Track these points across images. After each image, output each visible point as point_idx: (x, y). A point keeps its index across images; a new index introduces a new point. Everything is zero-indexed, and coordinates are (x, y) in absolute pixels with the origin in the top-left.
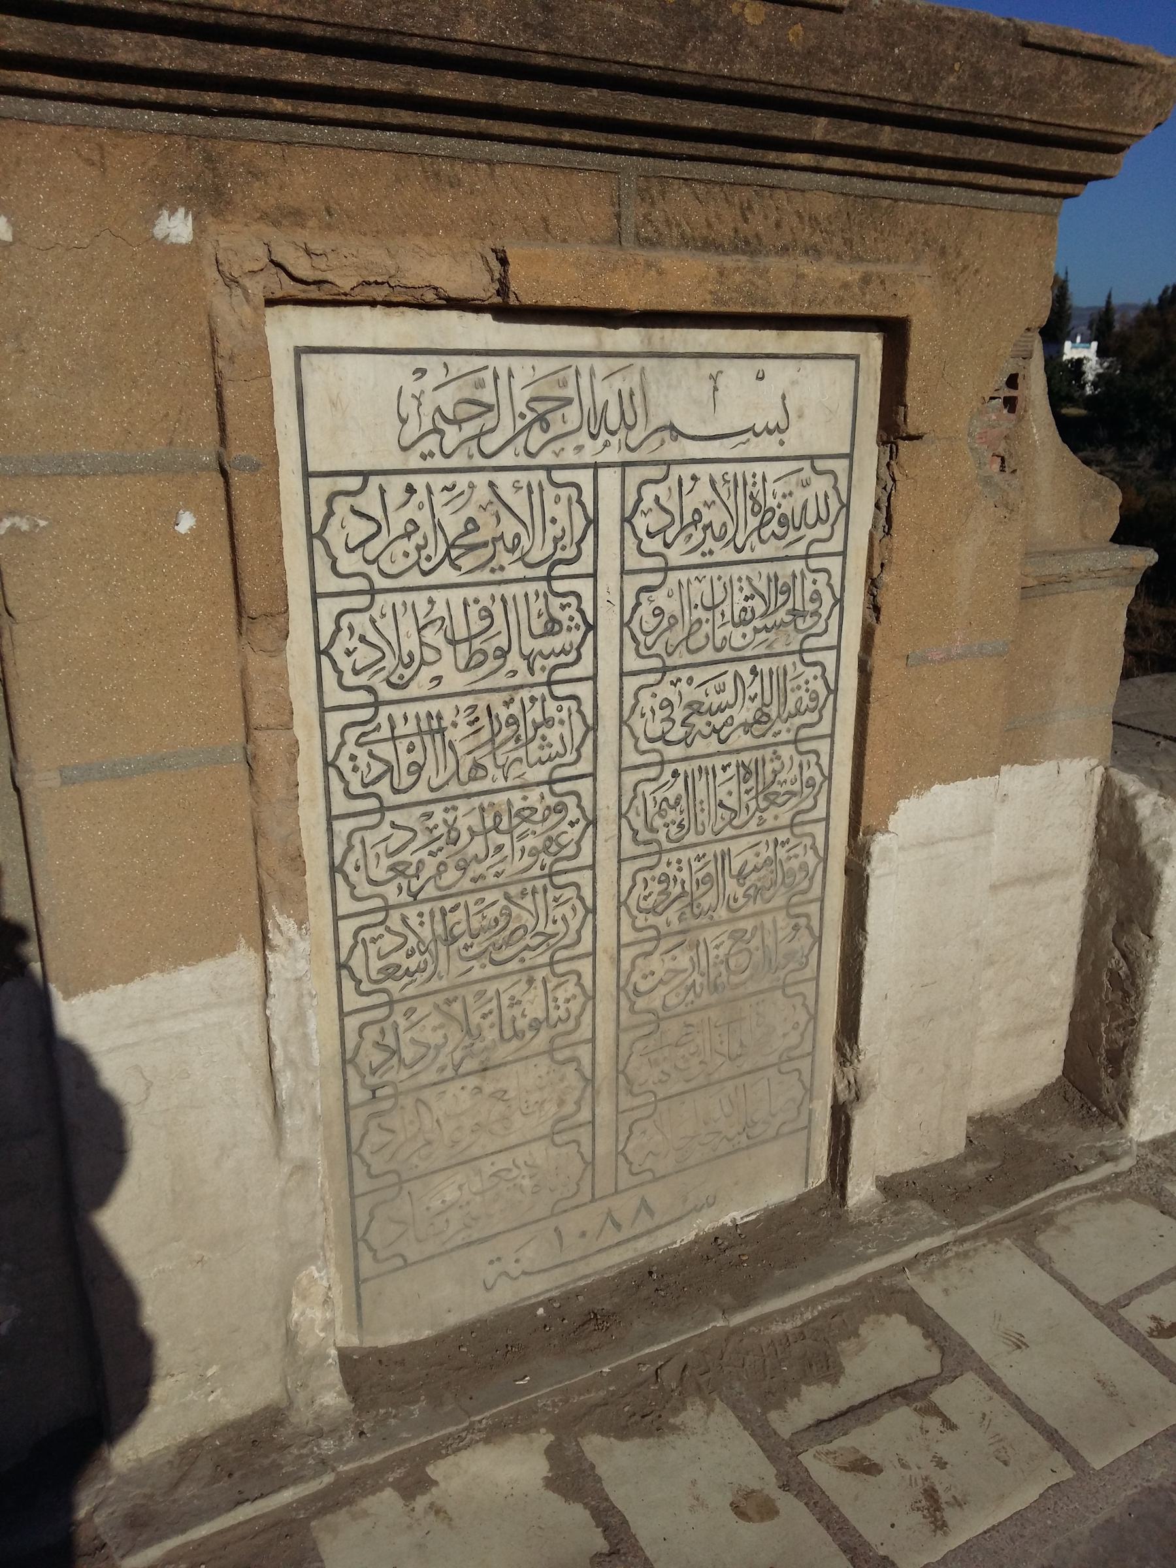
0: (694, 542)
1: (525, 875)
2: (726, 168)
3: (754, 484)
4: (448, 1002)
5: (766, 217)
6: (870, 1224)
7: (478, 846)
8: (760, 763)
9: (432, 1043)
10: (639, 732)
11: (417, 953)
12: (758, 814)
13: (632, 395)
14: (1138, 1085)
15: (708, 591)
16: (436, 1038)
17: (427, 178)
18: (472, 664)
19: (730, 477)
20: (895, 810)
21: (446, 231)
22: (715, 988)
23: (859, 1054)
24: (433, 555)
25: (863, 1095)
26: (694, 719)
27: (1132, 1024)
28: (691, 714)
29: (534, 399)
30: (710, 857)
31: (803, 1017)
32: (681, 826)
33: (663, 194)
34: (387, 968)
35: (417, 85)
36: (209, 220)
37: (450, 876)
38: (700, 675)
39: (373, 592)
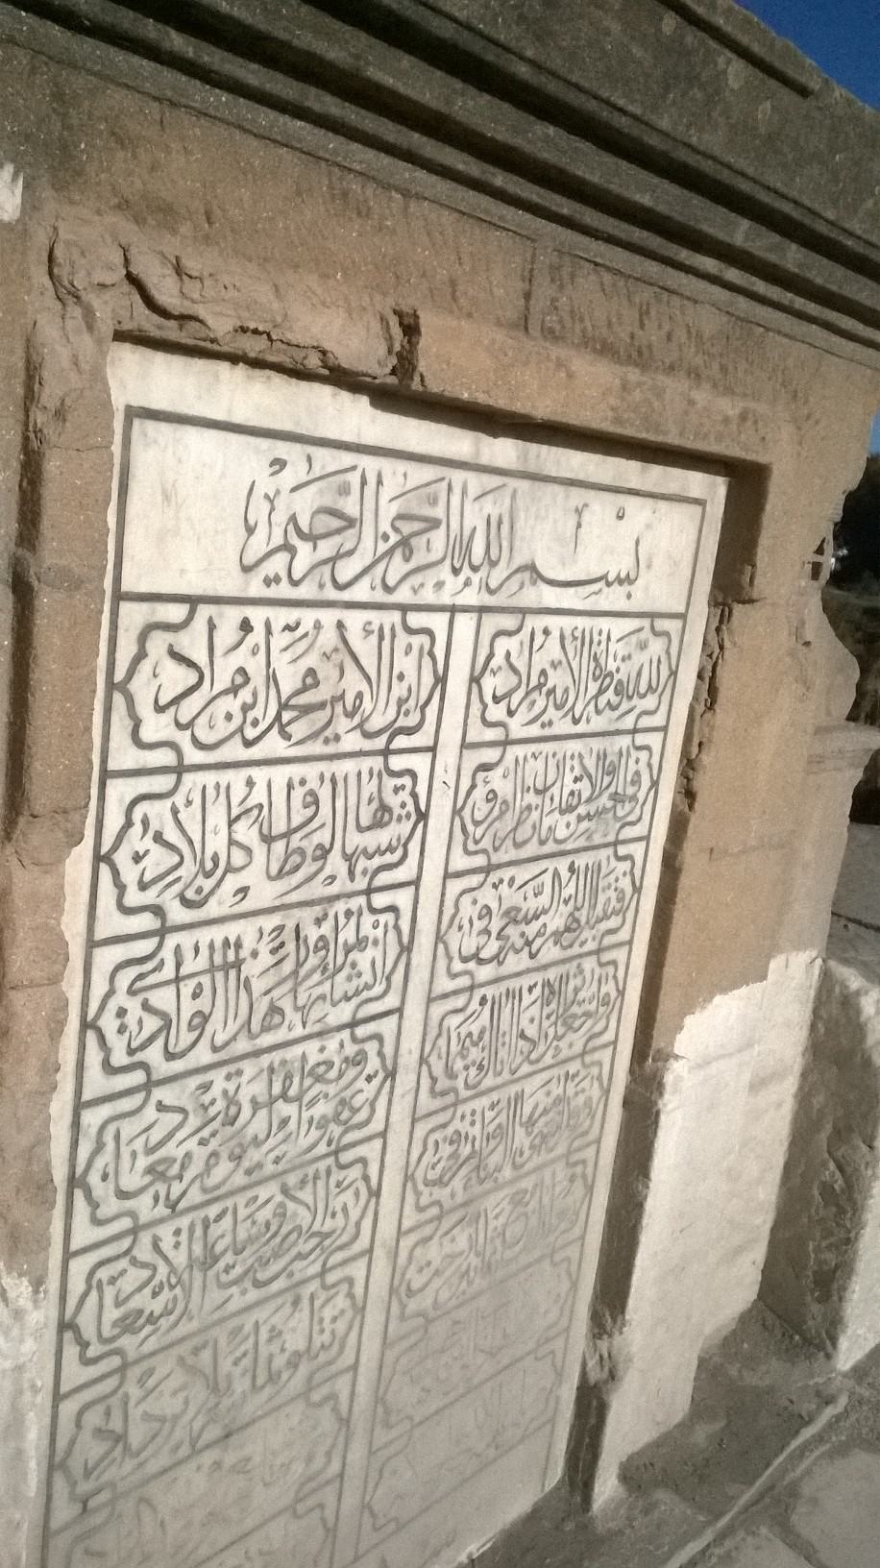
0: (537, 710)
1: (309, 1156)
2: (637, 258)
3: (599, 643)
4: (196, 1351)
5: (660, 327)
6: (621, 1532)
8: (564, 979)
9: (168, 1412)
11: (166, 1289)
12: (555, 1043)
13: (500, 523)
14: (849, 1311)
15: (541, 772)
17: (333, 197)
18: (287, 868)
19: (578, 634)
21: (345, 274)
23: (623, 1325)
24: (260, 719)
25: (620, 1373)
26: (511, 930)
27: (846, 1243)
28: (507, 925)
29: (400, 517)
30: (503, 1104)
31: (565, 1285)
32: (480, 1067)
33: (573, 276)
34: (124, 1318)
35: (368, 64)
36: (48, 193)
37: (223, 1168)
38: (522, 874)
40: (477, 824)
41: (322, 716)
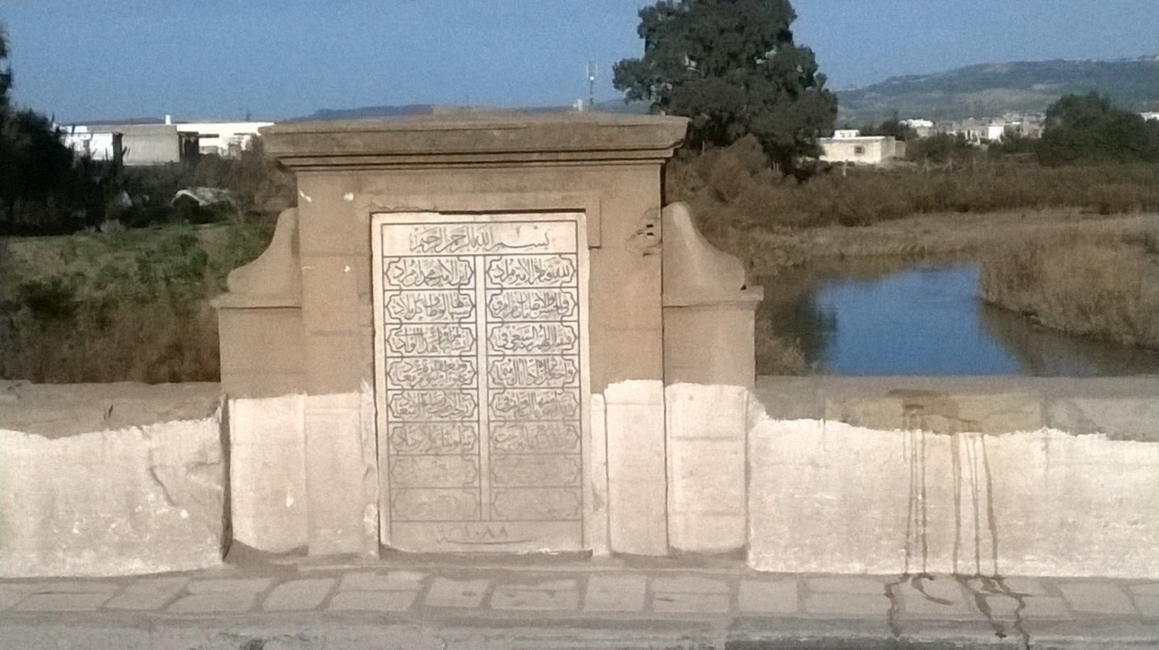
0: (513, 280)
4: (425, 427)
7: (434, 374)
10: (494, 343)
20: (607, 387)
22: (532, 447)
26: (516, 341)
32: (513, 380)
37: (424, 383)
39: (401, 290)
40: (496, 310)
41: (438, 280)
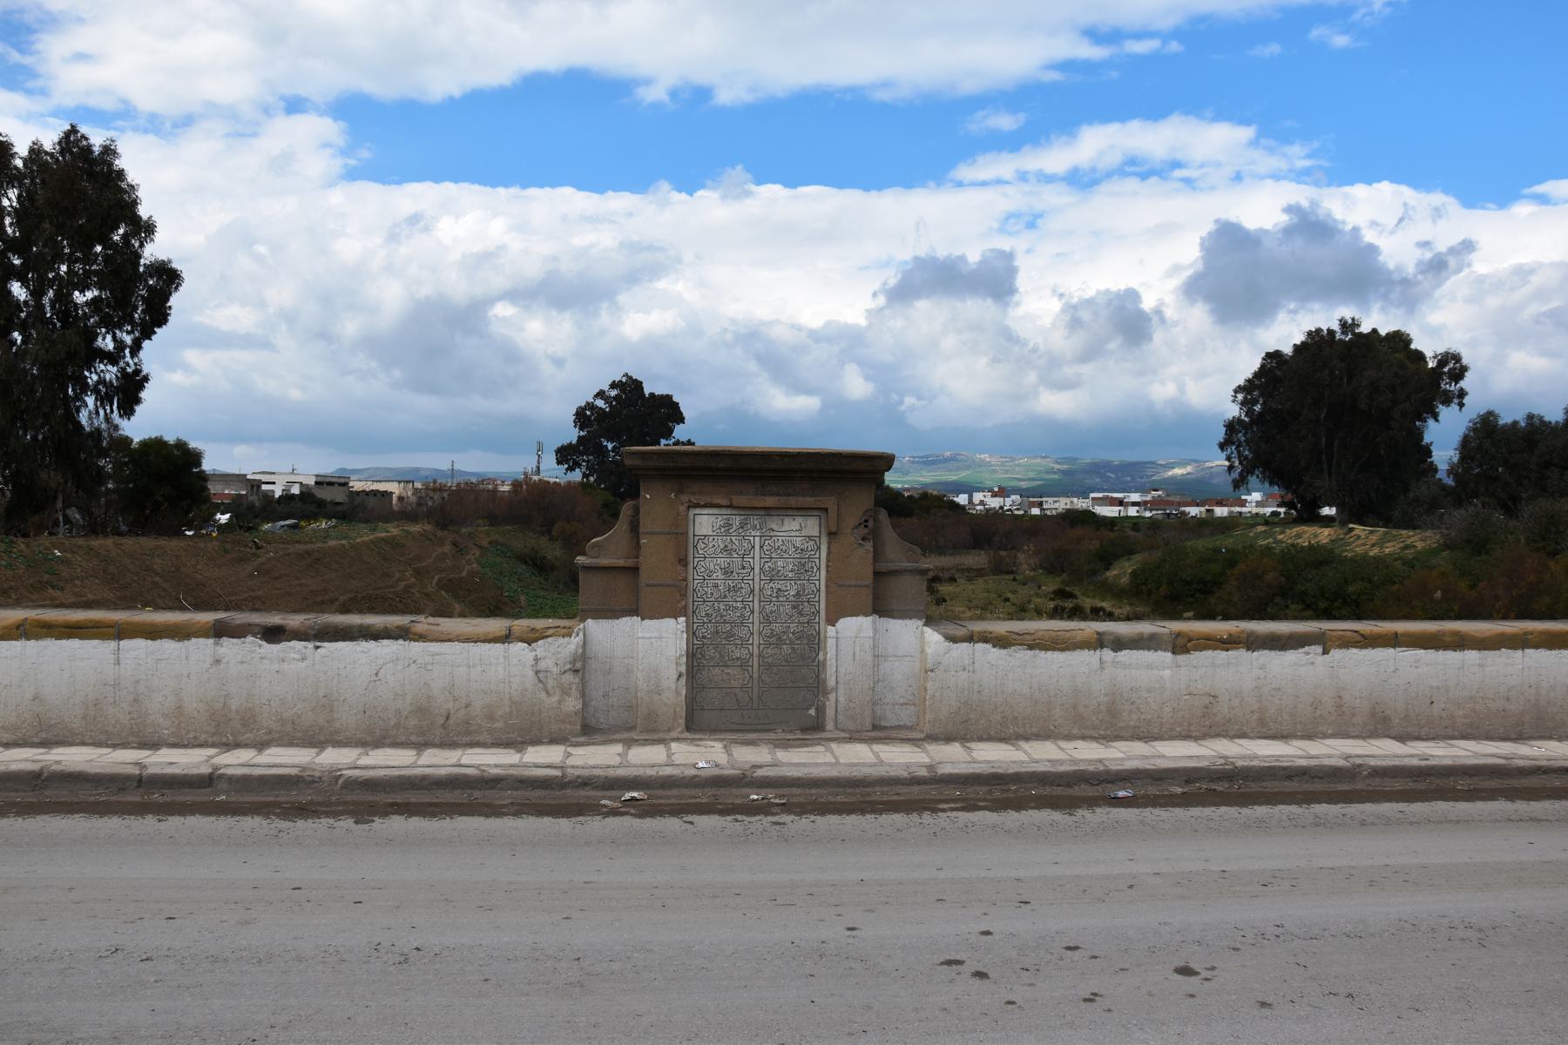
7: (725, 613)
8: (798, 605)
16: (713, 655)
22: (786, 661)
37: (718, 618)
